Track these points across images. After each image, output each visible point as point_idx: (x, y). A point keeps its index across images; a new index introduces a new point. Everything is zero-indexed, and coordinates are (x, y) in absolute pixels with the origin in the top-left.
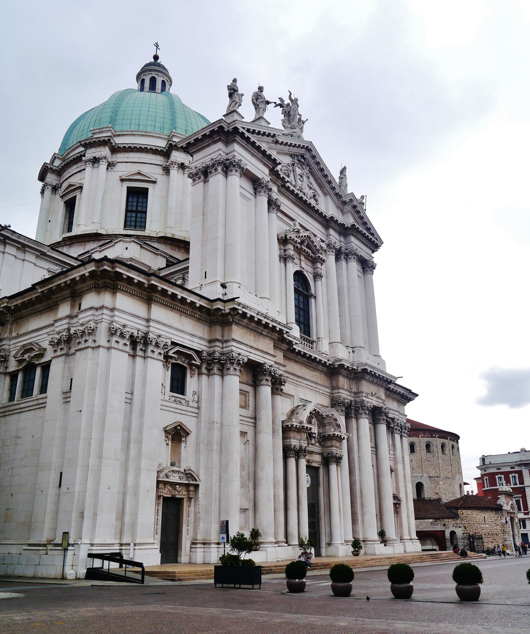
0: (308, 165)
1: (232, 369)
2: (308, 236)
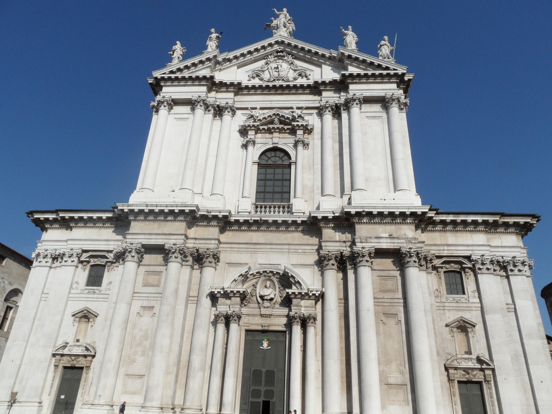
0: (289, 55)
1: (130, 256)
2: (274, 114)
